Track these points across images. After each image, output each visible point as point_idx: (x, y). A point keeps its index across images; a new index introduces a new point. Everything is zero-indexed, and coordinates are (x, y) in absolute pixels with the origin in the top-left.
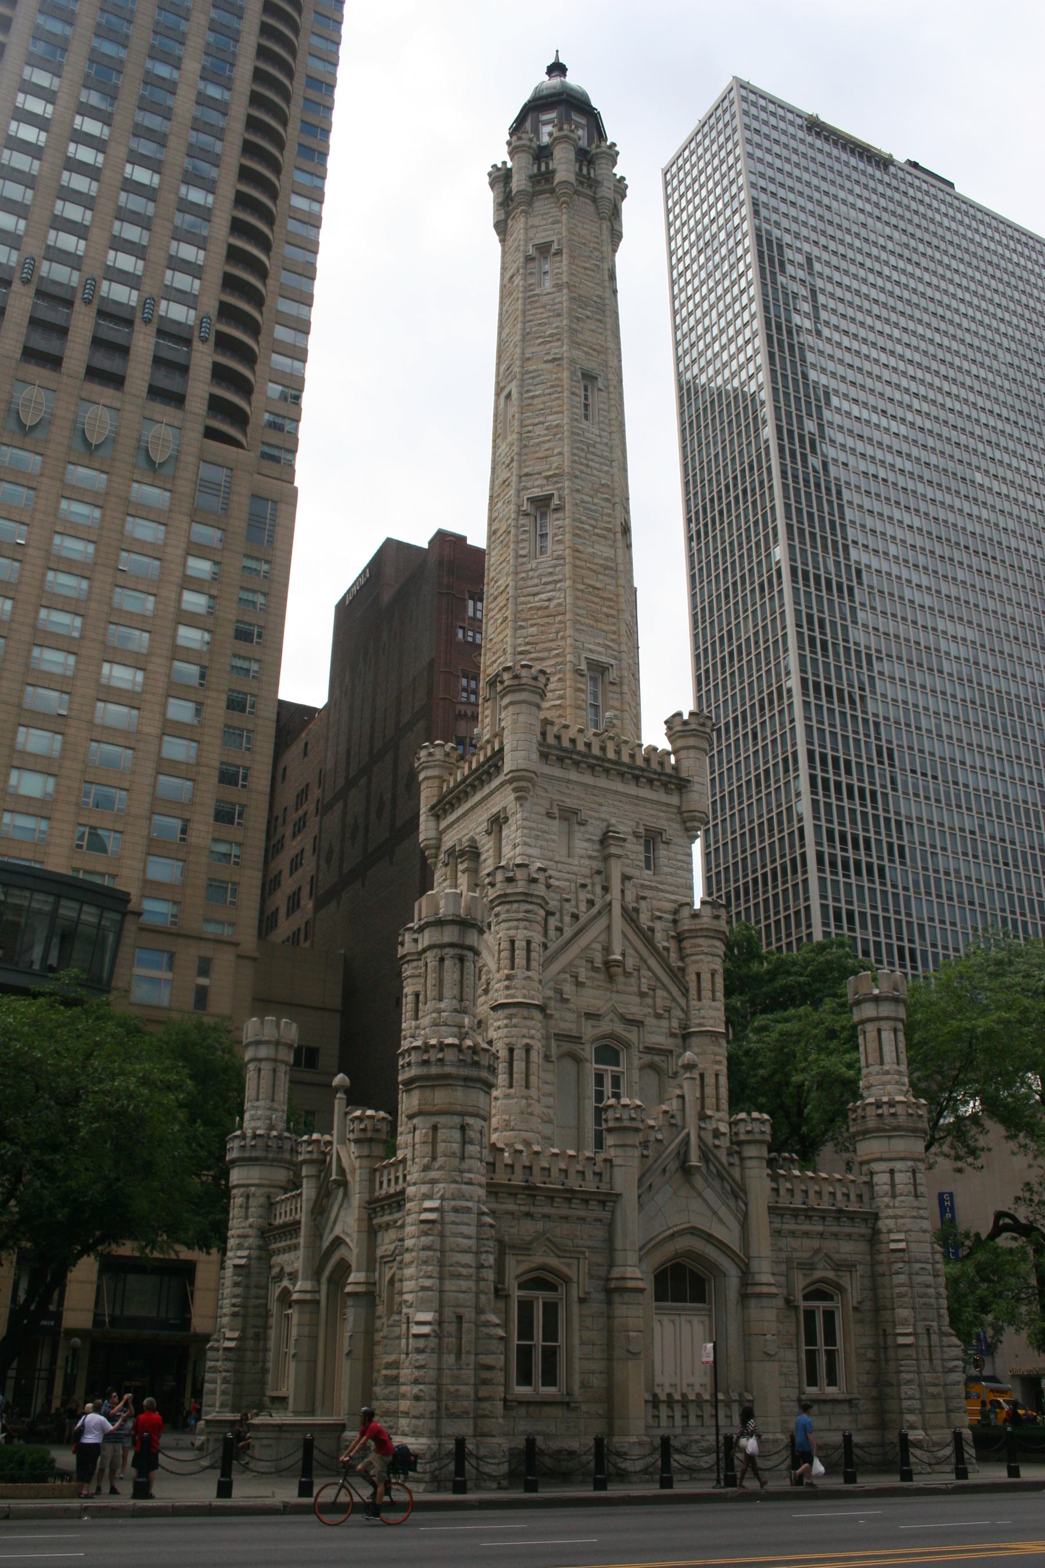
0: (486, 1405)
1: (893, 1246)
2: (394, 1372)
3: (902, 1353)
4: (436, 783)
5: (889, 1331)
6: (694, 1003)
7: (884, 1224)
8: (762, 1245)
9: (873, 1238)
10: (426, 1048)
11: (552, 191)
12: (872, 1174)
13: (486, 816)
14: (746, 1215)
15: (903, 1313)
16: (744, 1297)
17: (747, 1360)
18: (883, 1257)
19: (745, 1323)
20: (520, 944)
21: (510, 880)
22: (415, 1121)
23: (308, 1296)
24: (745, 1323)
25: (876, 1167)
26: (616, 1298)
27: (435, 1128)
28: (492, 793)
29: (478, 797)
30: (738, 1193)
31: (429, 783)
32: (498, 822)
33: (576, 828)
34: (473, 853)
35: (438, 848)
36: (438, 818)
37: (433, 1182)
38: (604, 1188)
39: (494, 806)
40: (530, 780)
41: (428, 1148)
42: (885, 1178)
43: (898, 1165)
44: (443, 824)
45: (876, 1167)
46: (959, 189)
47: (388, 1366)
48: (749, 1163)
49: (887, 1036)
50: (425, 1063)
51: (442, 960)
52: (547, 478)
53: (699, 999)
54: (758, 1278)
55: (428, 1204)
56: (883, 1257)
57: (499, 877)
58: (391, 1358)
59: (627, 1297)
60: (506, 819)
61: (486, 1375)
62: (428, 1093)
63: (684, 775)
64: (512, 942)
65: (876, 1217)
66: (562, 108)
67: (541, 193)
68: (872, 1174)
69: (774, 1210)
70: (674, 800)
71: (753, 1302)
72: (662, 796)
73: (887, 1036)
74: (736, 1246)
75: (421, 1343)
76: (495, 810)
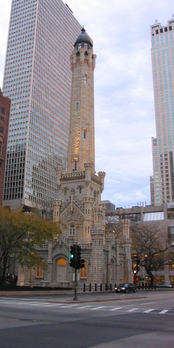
0: (104, 280)
1: (128, 259)
2: (92, 275)
3: (129, 274)
4: (61, 174)
5: (126, 270)
6: (102, 220)
7: (126, 256)
8: (118, 259)
9: (125, 258)
10: (99, 230)
11: (87, 63)
12: (125, 249)
13: (76, 185)
14: (117, 254)
15: (129, 268)
16: (116, 265)
17: (116, 274)
18: (126, 261)
19: (116, 269)
20: (88, 210)
21: (89, 200)
22: (96, 240)
23: (52, 262)
24: (116, 269)
25: (126, 248)
26: (109, 265)
27: (99, 242)
28: (79, 181)
29: (74, 181)
30: (116, 251)
31: (59, 174)
32: (80, 188)
33: (92, 190)
34: (73, 191)
35: (60, 186)
36: (61, 180)
37: (100, 249)
38: (107, 250)
39: (80, 184)
40: (89, 182)
41: (98, 244)
42: (127, 249)
43: (129, 248)
44: (62, 182)
45: (126, 248)
46: (74, 14)
47: (91, 274)
48: (117, 247)
49: (128, 229)
50: (99, 232)
51: (99, 217)
52: (86, 124)
53: (103, 219)
54: (117, 263)
55: (99, 252)
56: (126, 261)
57: (88, 199)
58: (91, 273)
59: (110, 265)
60: (83, 188)
61: (104, 276)
62: (99, 236)
63: (102, 182)
64: (89, 210)
65: (125, 255)
66: (89, 44)
67: (86, 62)
68: (125, 249)
69: (120, 254)
70: (100, 186)
71: (117, 266)
72: (98, 185)
73: (128, 229)
74: (115, 257)
75: (101, 271)
76: (80, 185)
